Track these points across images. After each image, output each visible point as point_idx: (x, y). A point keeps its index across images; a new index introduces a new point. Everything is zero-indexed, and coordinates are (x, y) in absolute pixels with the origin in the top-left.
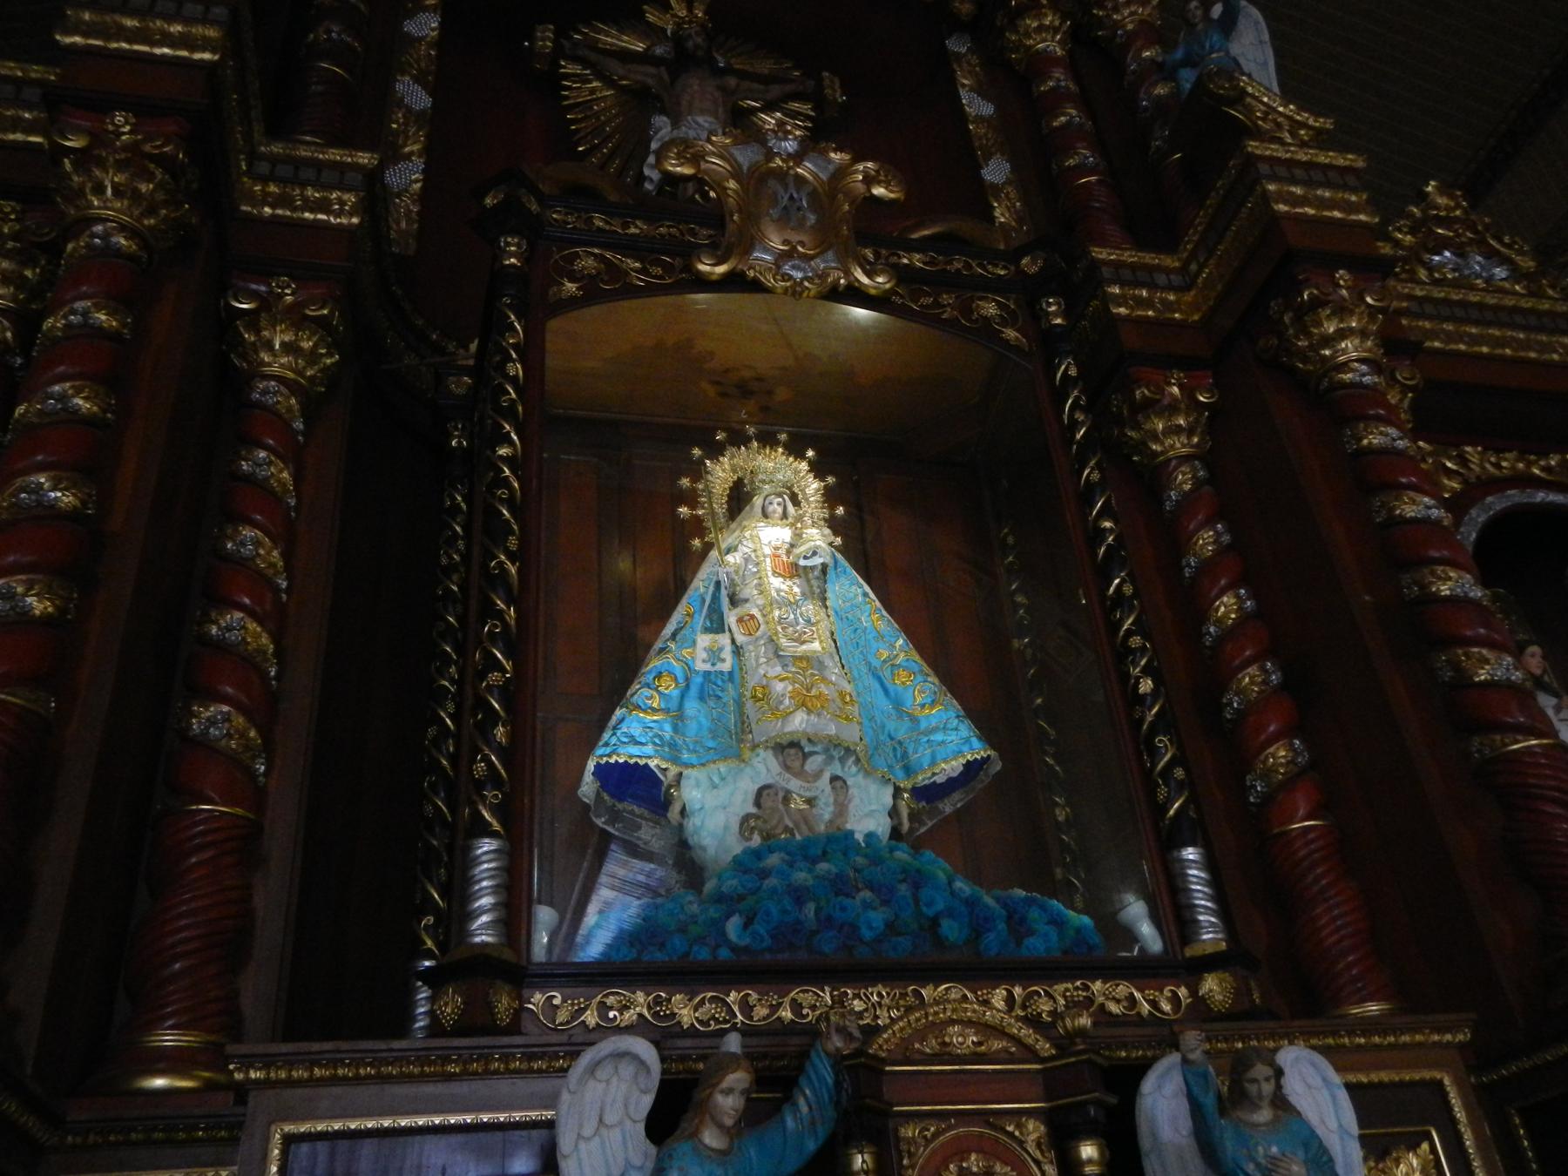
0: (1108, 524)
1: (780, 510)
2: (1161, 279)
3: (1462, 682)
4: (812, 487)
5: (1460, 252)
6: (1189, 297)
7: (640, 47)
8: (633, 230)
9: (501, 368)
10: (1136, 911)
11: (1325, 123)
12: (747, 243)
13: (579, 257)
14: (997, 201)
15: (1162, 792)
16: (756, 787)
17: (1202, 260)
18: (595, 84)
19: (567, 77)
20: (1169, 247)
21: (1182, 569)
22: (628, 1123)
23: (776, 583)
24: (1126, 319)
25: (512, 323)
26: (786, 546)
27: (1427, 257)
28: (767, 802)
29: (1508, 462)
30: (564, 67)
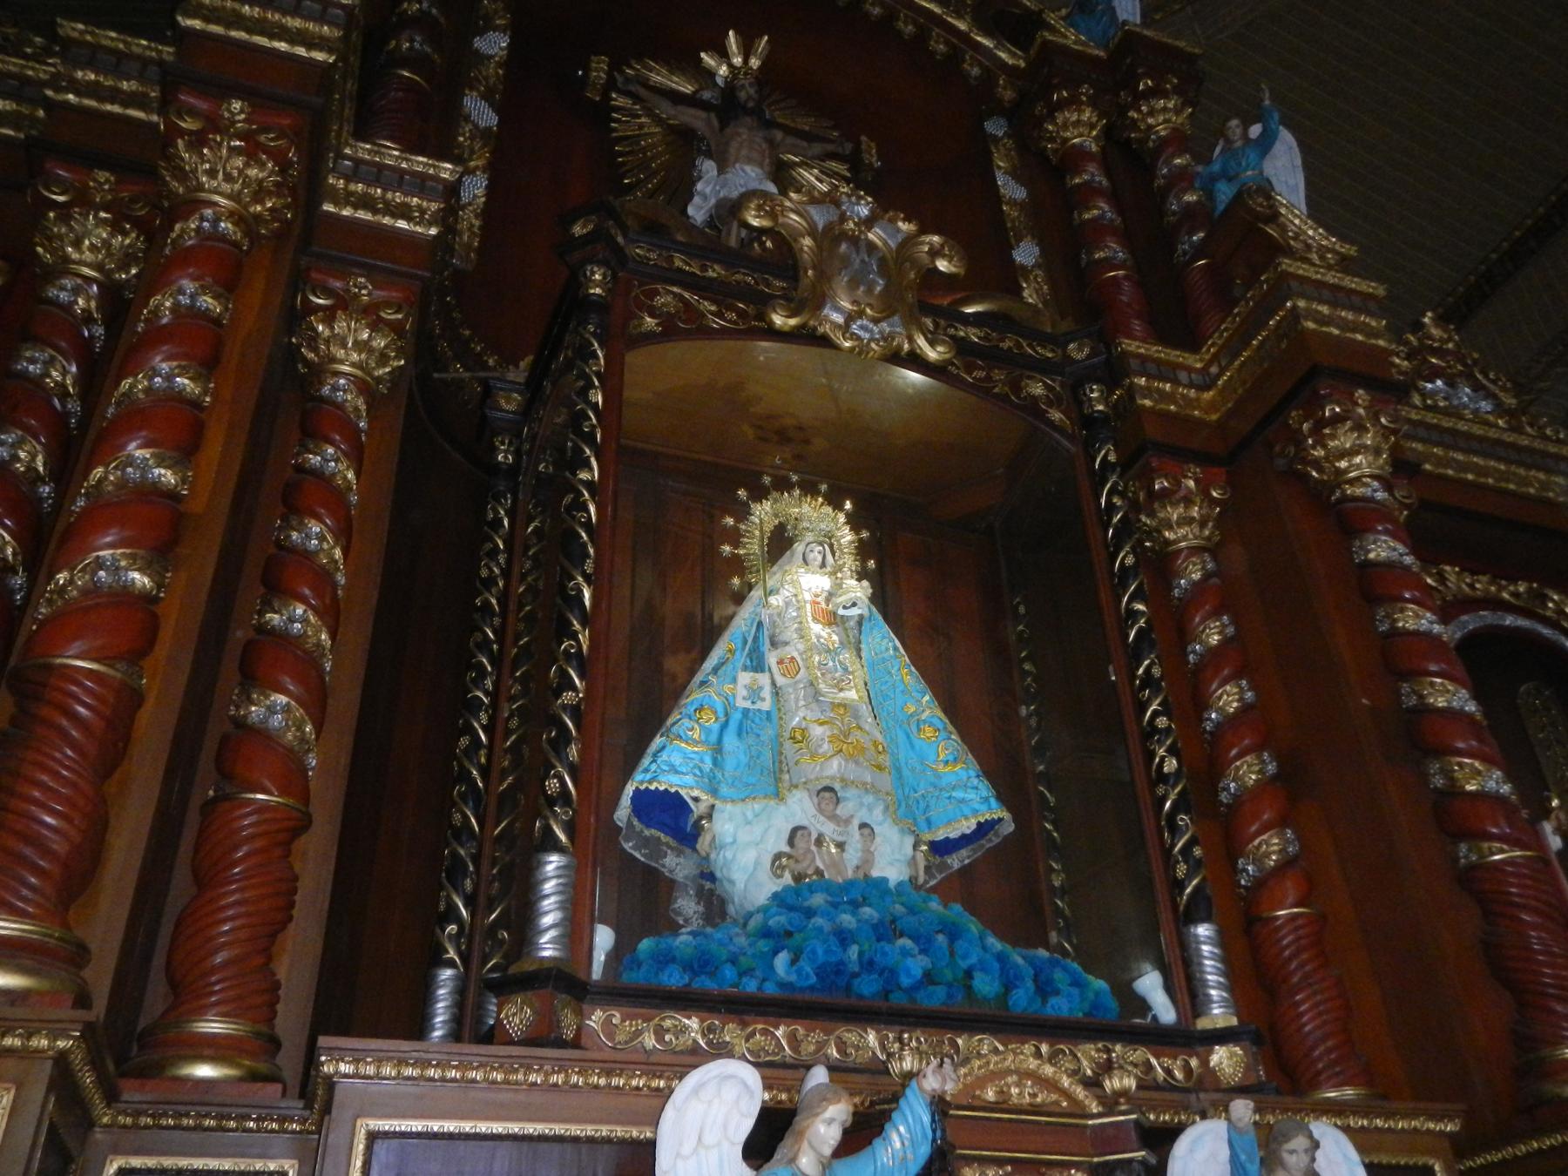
0: (1141, 607)
1: (820, 558)
2: (1183, 376)
3: (1453, 791)
4: (847, 536)
5: (1451, 383)
6: (1208, 395)
7: (688, 89)
8: (711, 274)
9: (583, 393)
10: (1150, 984)
11: (1350, 249)
12: (817, 301)
13: (659, 294)
14: (1026, 282)
15: (1181, 870)
16: (790, 827)
17: (1223, 364)
18: (643, 120)
19: (618, 109)
20: (1194, 347)
21: (1186, 655)
22: (726, 1145)
23: (816, 628)
24: (1151, 410)
25: (595, 351)
26: (825, 594)
27: (1421, 383)
28: (798, 840)
29: (1482, 584)
30: (615, 100)
